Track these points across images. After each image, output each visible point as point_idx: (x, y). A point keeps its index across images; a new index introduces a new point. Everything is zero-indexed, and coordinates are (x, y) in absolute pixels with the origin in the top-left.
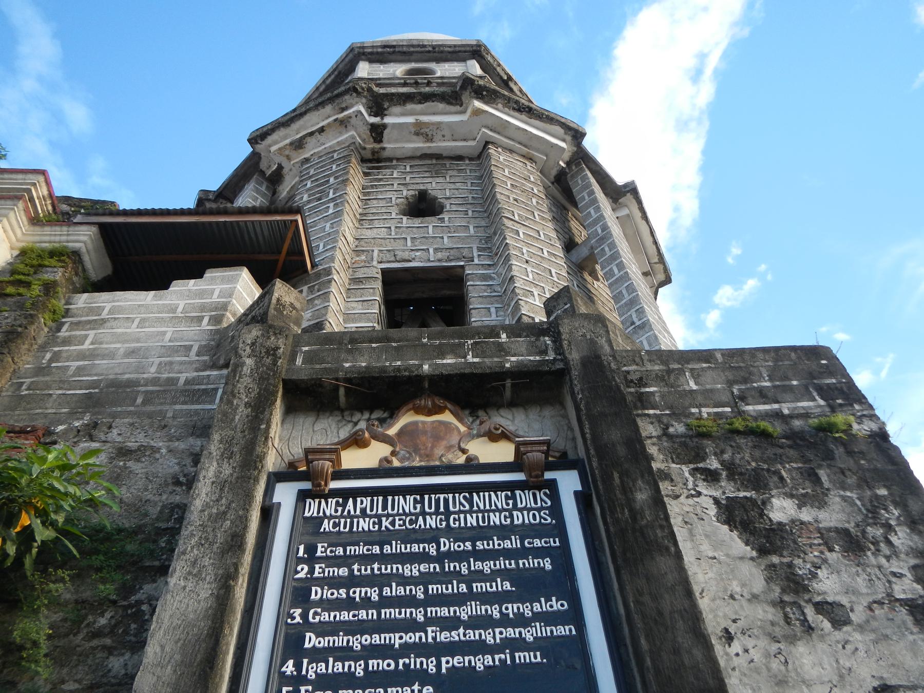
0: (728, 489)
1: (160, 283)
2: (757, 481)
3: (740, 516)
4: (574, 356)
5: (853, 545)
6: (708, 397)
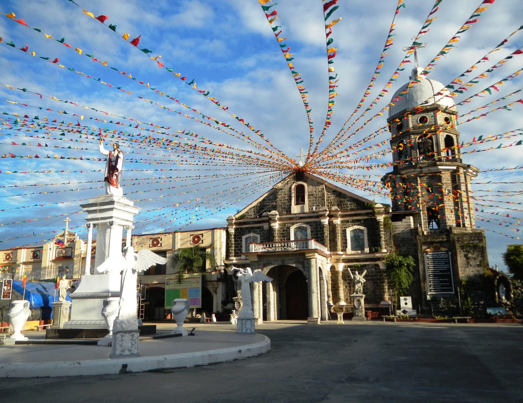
0: (466, 253)
1: (400, 220)
2: (468, 252)
3: (466, 256)
4: (451, 240)
5: (475, 259)
6: (466, 240)
